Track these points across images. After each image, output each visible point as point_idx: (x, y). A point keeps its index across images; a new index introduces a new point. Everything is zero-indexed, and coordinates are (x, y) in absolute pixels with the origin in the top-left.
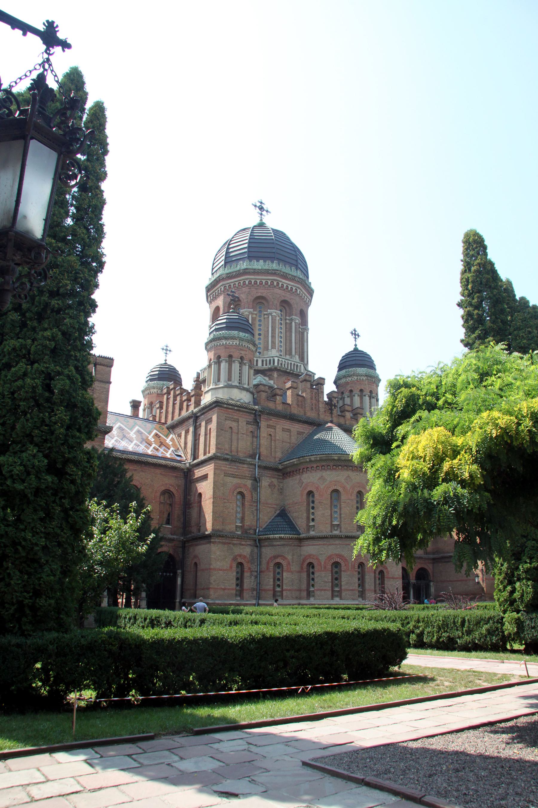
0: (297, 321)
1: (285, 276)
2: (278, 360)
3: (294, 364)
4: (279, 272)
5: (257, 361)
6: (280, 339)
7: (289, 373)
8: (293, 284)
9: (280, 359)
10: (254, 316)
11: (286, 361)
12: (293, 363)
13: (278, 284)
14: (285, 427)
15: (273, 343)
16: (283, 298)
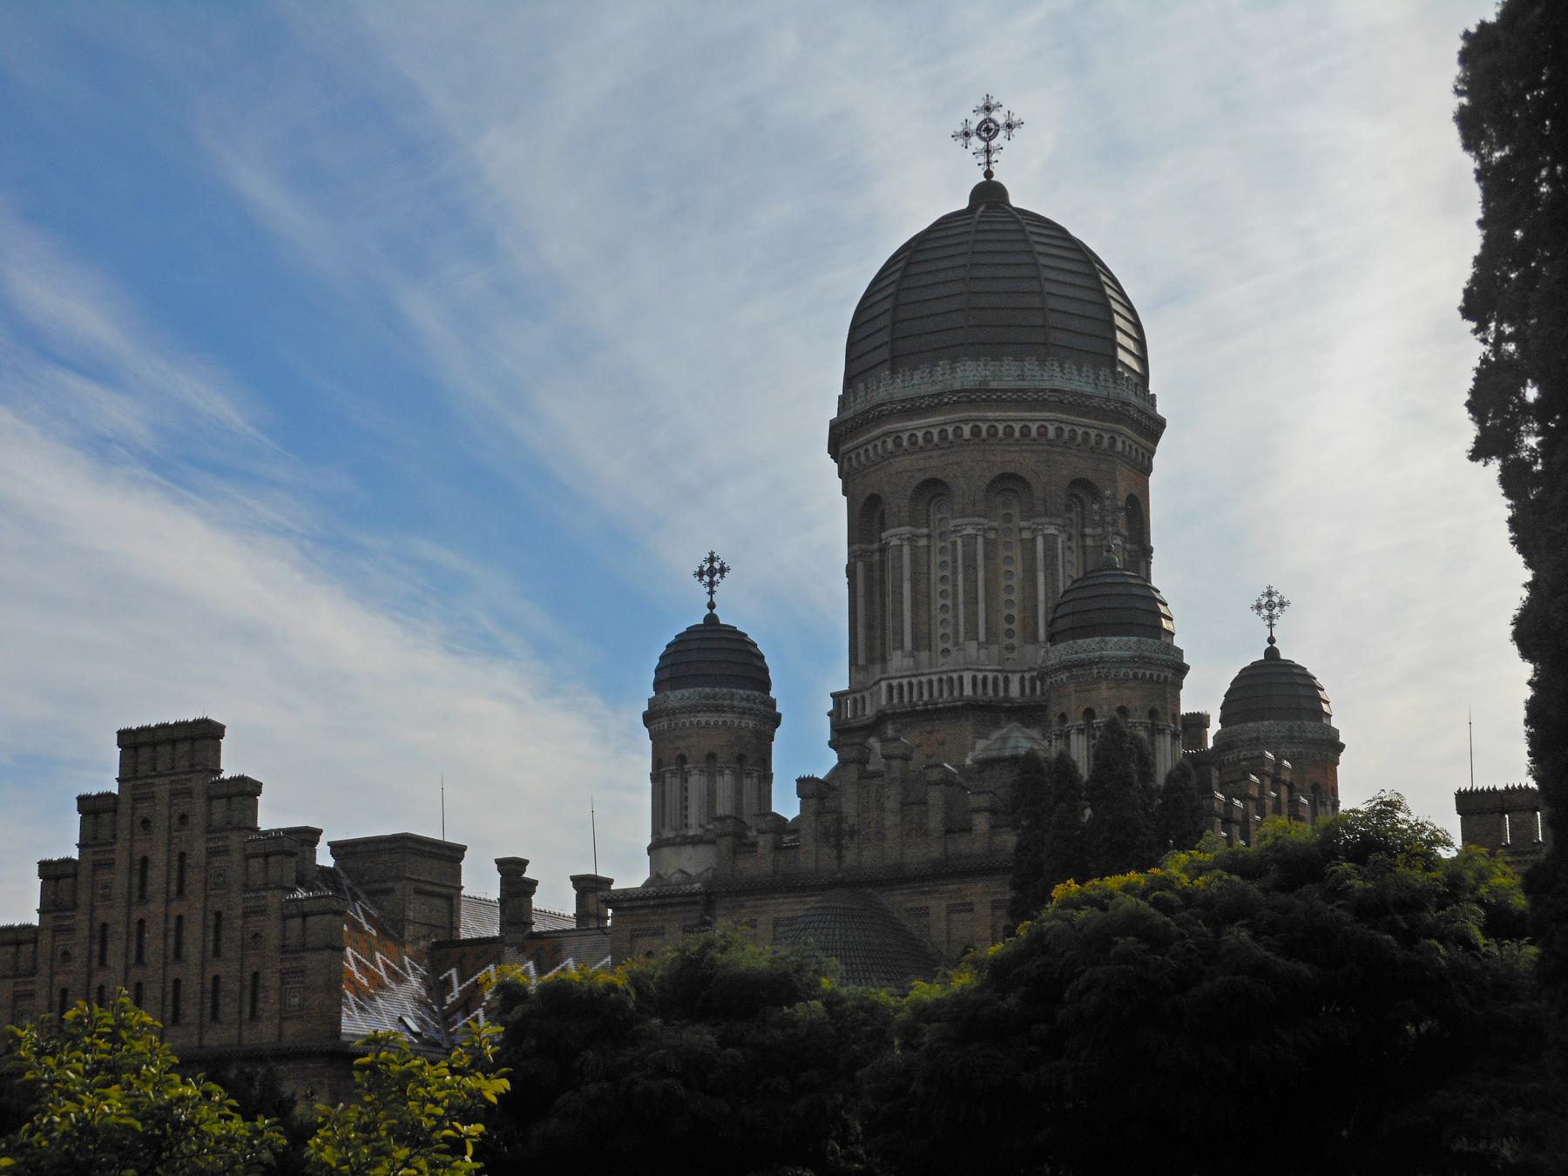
0: (969, 530)
1: (912, 408)
2: (890, 687)
3: (941, 680)
4: (889, 407)
5: (863, 698)
6: (949, 602)
7: (926, 711)
8: (941, 418)
9: (895, 683)
10: (877, 557)
11: (914, 681)
12: (934, 678)
13: (898, 444)
14: (782, 915)
15: (899, 632)
16: (920, 477)
